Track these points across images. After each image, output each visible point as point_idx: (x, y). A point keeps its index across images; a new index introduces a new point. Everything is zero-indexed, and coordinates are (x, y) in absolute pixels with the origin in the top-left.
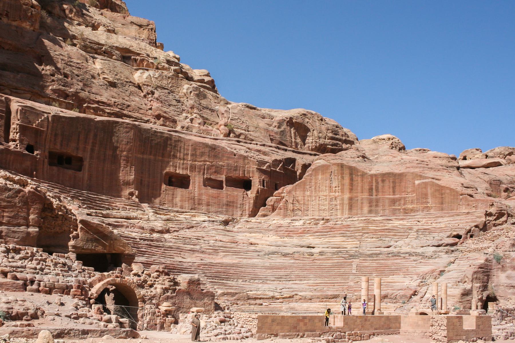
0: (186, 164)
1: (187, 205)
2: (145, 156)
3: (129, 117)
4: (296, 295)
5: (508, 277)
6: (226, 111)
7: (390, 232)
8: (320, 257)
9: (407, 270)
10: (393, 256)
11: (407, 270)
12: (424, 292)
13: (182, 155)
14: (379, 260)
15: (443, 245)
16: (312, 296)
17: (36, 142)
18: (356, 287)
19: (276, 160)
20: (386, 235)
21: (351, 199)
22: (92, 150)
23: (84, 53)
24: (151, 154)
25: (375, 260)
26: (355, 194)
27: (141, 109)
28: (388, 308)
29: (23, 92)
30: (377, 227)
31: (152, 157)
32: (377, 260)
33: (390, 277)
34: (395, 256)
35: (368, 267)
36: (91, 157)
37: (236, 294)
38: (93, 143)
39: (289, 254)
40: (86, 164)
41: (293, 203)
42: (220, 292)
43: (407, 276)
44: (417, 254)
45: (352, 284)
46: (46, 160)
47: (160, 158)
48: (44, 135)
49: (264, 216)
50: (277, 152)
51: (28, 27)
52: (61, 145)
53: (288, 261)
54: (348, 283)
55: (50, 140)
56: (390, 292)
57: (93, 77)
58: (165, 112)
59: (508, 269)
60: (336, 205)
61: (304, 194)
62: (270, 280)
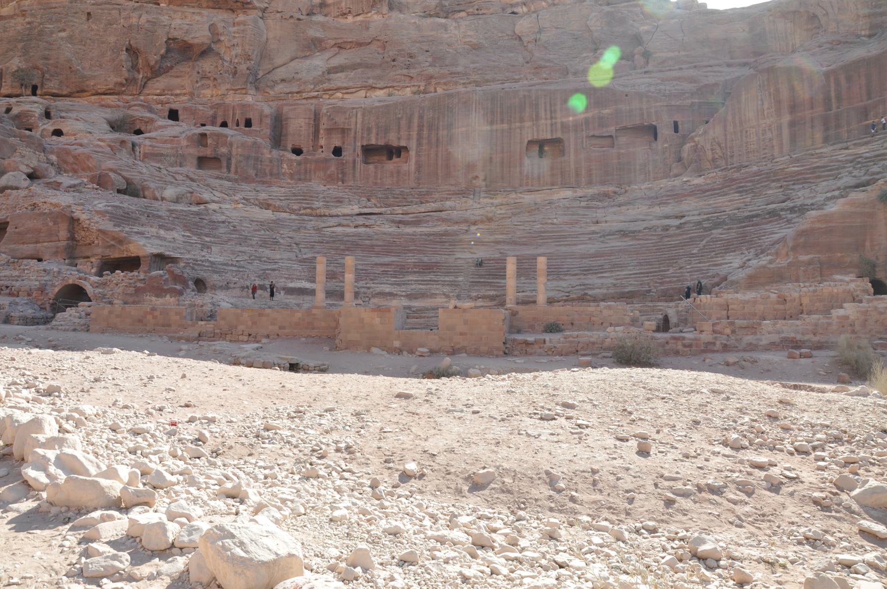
0: (556, 123)
1: (560, 179)
2: (494, 127)
3: (494, 80)
4: (586, 294)
6: (647, 32)
8: (677, 232)
13: (548, 112)
16: (606, 294)
17: (344, 143)
19: (706, 86)
20: (805, 179)
21: (792, 124)
22: (420, 137)
23: (443, 21)
24: (502, 122)
26: (799, 114)
27: (513, 66)
29: (354, 90)
30: (802, 166)
31: (506, 126)
34: (774, 216)
36: (419, 144)
37: (497, 296)
38: (419, 126)
39: (634, 232)
40: (413, 153)
41: (712, 150)
42: (474, 294)
46: (359, 160)
47: (518, 124)
48: (353, 132)
49: (676, 176)
50: (719, 72)
51: (375, 17)
52: (377, 139)
53: (627, 242)
55: (362, 137)
57: (449, 45)
58: (549, 61)
60: (770, 140)
61: (725, 130)
62: (570, 274)
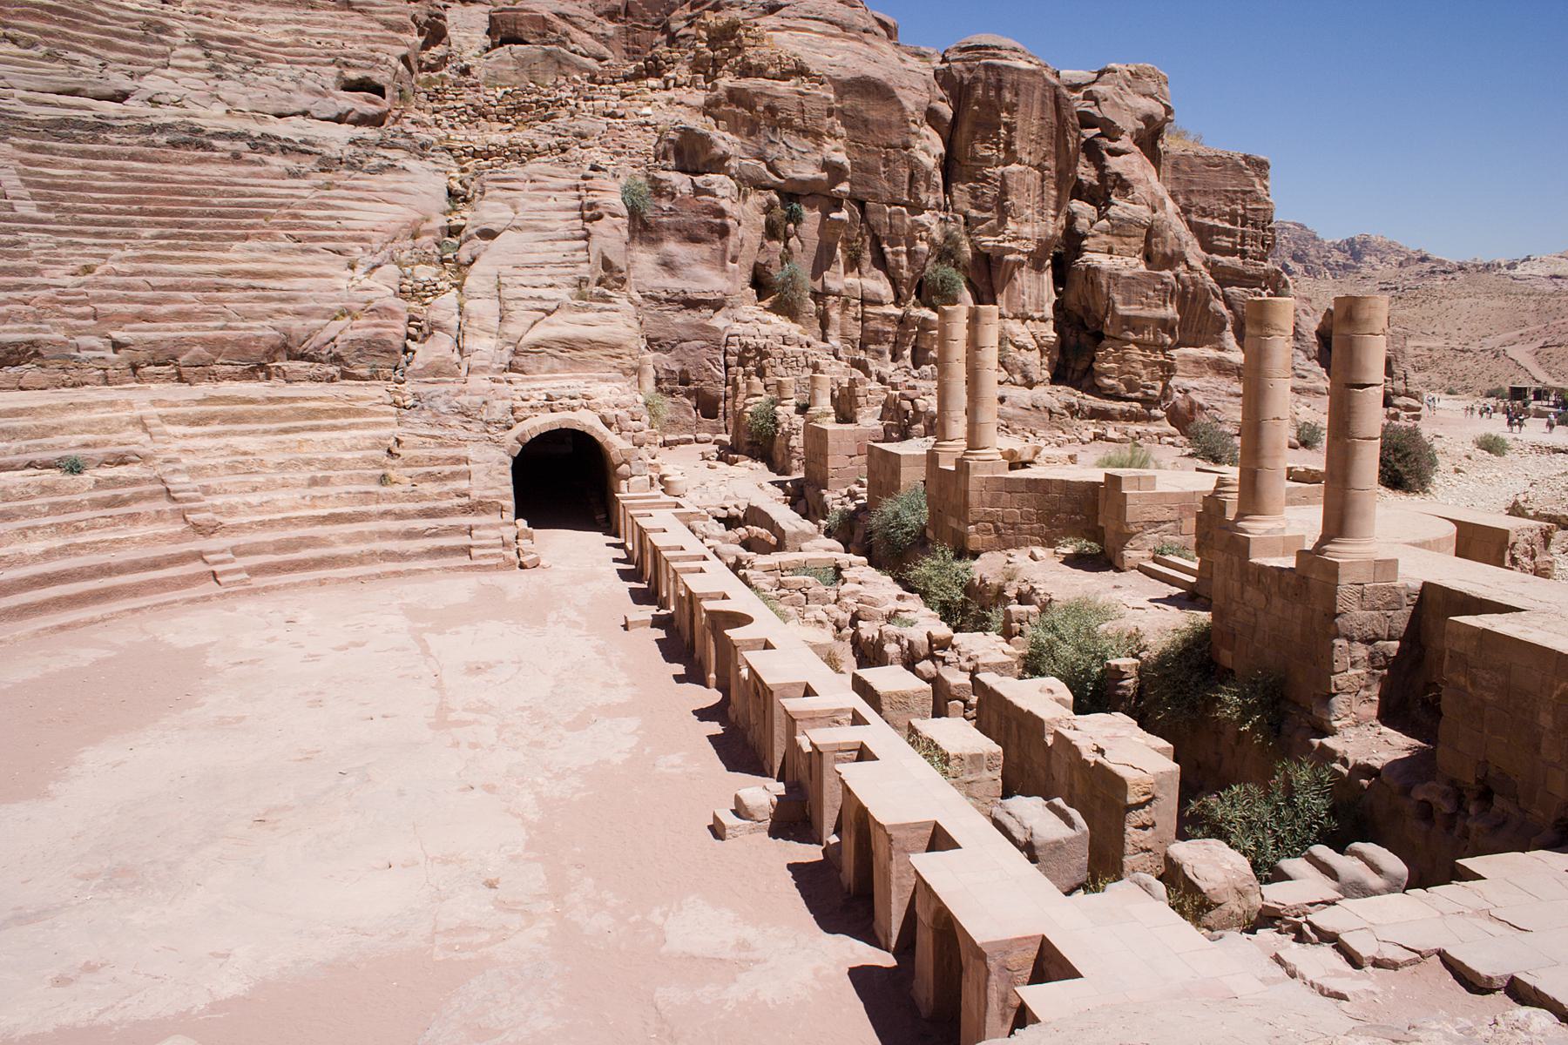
5: (668, 265)
7: (76, 26)
9: (295, 216)
10: (174, 145)
11: (295, 216)
12: (453, 322)
14: (117, 157)
15: (350, 117)
18: (102, 300)
25: (94, 155)
28: (359, 413)
32: (104, 155)
33: (237, 245)
34: (186, 143)
35: (79, 188)
43: (317, 246)
44: (287, 148)
45: (60, 276)
54: (35, 271)
56: (297, 324)
59: (665, 234)
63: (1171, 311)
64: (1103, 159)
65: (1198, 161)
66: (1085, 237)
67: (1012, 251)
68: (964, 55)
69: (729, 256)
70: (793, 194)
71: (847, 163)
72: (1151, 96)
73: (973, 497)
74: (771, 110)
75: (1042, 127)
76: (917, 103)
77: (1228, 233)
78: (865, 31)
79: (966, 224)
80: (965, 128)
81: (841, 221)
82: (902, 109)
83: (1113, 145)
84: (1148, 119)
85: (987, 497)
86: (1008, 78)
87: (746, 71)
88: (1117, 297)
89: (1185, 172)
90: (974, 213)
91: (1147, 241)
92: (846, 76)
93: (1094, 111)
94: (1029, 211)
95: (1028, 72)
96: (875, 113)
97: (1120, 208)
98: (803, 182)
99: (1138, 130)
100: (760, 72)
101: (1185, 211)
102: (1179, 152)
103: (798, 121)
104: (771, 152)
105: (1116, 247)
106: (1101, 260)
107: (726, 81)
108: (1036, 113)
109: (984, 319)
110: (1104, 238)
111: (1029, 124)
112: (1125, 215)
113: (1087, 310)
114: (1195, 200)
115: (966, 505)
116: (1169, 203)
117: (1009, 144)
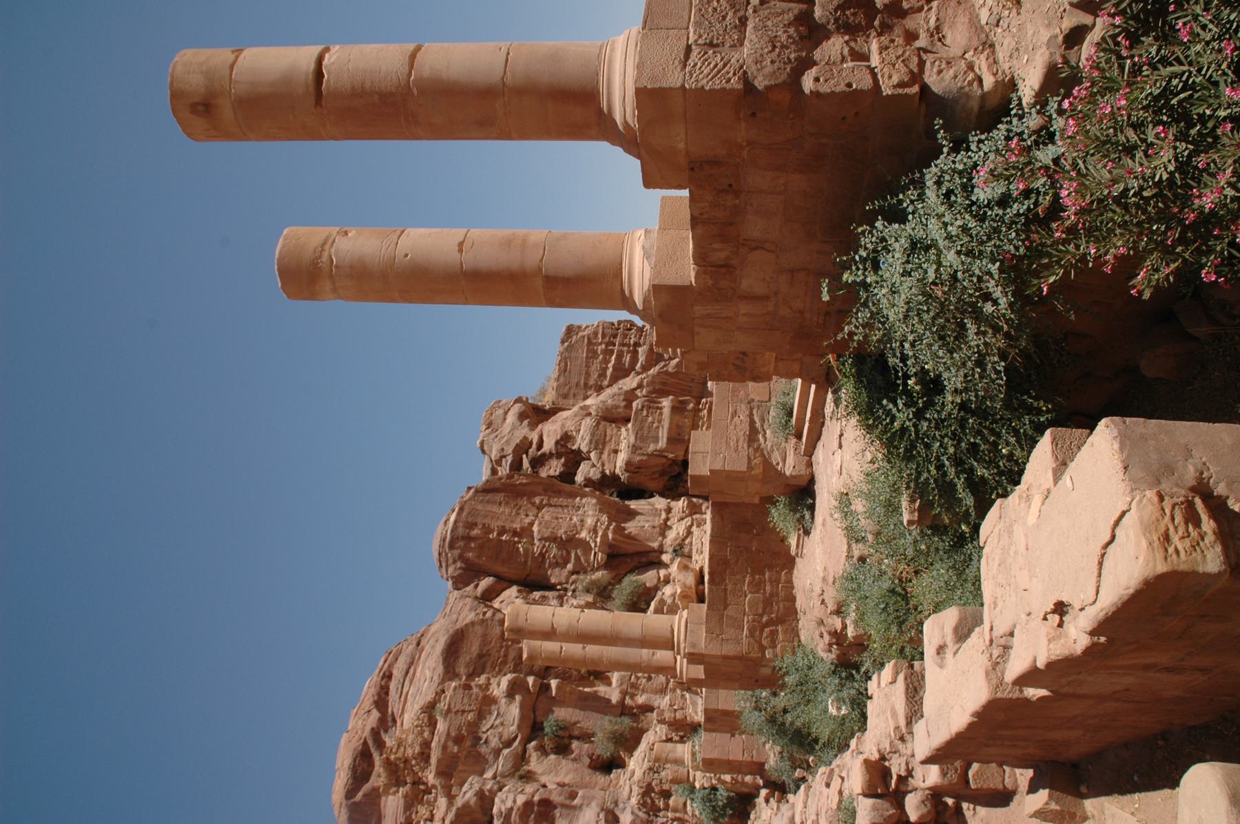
63: (666, 403)
64: (544, 455)
65: (562, 379)
66: (603, 472)
67: (605, 535)
68: (444, 565)
69: (567, 802)
70: (533, 728)
71: (509, 676)
72: (506, 413)
73: (729, 649)
74: (459, 740)
75: (507, 503)
76: (471, 610)
77: (620, 356)
78: (418, 644)
79: (578, 573)
80: (499, 568)
81: (558, 688)
82: (473, 623)
83: (534, 446)
84: (522, 416)
85: (730, 633)
86: (461, 531)
87: (424, 756)
88: (652, 448)
89: (570, 389)
90: (570, 566)
91: (612, 421)
92: (440, 669)
93: (510, 459)
94: (575, 519)
95: (459, 514)
96: (472, 648)
97: (582, 443)
98: (523, 717)
99: (529, 424)
100: (426, 745)
101: (599, 389)
102: (554, 393)
103: (470, 717)
104: (494, 742)
105: (613, 447)
106: (622, 458)
107: (430, 777)
108: (495, 508)
109: (521, 623)
110: (605, 456)
111: (501, 515)
112: (587, 441)
113: (663, 473)
114: (591, 382)
115: (739, 658)
116: (588, 402)
117: (515, 533)
